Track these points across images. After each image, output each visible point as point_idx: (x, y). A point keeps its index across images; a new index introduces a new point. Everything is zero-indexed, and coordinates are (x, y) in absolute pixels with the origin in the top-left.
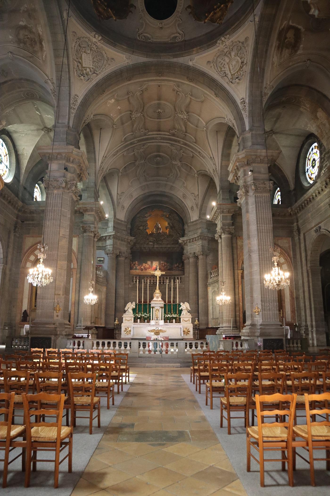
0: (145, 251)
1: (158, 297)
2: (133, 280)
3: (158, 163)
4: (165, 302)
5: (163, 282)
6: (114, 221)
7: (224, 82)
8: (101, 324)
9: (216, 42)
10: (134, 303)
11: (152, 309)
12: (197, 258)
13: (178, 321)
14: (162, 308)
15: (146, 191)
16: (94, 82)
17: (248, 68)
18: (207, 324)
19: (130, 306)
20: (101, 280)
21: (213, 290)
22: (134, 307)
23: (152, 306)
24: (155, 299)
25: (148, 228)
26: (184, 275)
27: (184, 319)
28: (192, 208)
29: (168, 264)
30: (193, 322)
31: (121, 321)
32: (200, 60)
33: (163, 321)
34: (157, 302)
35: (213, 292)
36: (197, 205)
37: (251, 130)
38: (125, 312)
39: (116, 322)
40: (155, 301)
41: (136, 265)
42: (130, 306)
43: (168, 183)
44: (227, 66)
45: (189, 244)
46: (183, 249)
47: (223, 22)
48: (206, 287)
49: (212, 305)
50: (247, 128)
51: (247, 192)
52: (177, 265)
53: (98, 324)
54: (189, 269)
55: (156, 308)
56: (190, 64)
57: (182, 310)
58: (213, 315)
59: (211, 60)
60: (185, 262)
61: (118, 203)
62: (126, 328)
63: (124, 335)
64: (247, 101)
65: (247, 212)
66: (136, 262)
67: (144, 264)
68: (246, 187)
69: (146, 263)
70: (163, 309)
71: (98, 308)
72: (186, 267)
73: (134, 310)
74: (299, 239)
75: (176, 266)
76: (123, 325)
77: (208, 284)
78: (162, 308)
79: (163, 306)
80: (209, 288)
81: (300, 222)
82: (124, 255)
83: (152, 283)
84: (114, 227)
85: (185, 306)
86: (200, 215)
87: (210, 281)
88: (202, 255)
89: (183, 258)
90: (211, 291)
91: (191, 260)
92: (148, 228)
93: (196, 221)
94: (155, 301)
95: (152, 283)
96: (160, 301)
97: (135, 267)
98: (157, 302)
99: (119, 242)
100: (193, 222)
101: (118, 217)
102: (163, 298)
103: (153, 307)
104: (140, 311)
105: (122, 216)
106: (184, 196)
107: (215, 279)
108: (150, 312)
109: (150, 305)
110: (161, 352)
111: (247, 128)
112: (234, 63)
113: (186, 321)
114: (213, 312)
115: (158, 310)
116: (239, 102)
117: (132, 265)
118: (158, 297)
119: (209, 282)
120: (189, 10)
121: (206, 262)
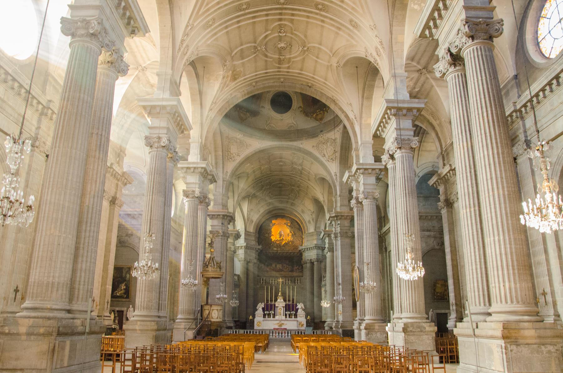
3: (280, 187)
6: (245, 234)
7: (323, 160)
9: (317, 136)
10: (263, 304)
12: (312, 263)
13: (296, 316)
15: (271, 206)
16: (238, 161)
17: (338, 155)
19: (260, 306)
23: (276, 305)
24: (278, 300)
25: (273, 235)
26: (302, 276)
28: (309, 222)
30: (306, 317)
31: (254, 317)
32: (307, 145)
34: (280, 303)
36: (313, 220)
37: (340, 196)
38: (257, 310)
39: (251, 317)
42: (260, 306)
43: (290, 200)
44: (325, 150)
45: (307, 252)
46: (301, 255)
47: (322, 122)
48: (320, 288)
50: (338, 193)
51: (336, 237)
54: (307, 273)
56: (301, 146)
57: (298, 309)
59: (315, 145)
61: (248, 219)
63: (256, 327)
64: (338, 174)
65: (336, 250)
68: (336, 234)
72: (304, 270)
73: (263, 309)
74: (386, 255)
76: (255, 320)
81: (387, 243)
84: (245, 239)
85: (300, 306)
86: (315, 227)
88: (317, 261)
91: (308, 265)
92: (273, 235)
93: (312, 233)
98: (280, 303)
99: (248, 251)
100: (310, 233)
101: (248, 230)
102: (285, 300)
105: (251, 229)
106: (303, 212)
109: (275, 305)
110: (282, 336)
111: (338, 193)
112: (329, 149)
116: (333, 174)
120: (301, 109)
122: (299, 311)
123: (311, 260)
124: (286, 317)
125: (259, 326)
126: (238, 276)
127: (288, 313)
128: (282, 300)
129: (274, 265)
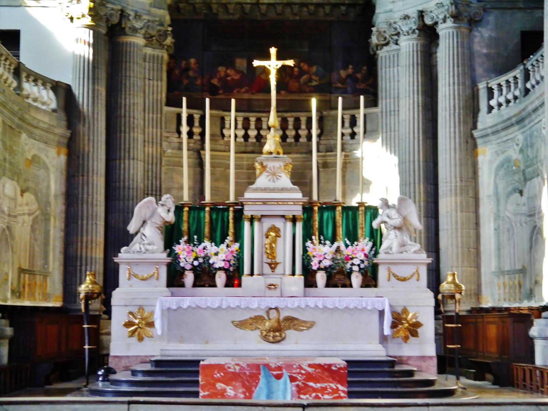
0: (226, 17)
1: (274, 175)
2: (179, 123)
4: (308, 193)
5: (297, 137)
8: (46, 297)
11: (246, 225)
12: (428, 34)
14: (294, 220)
18: (478, 294)
19: (149, 217)
20: (46, 119)
21: (501, 158)
22: (171, 217)
23: (248, 211)
24: (262, 181)
27: (396, 270)
29: (314, 69)
33: (299, 279)
35: (502, 165)
38: (127, 239)
40: (265, 190)
41: (191, 73)
48: (470, 146)
49: (497, 217)
52: (350, 71)
53: (32, 296)
55: (267, 223)
58: (499, 256)
60: (382, 53)
62: (135, 310)
63: (120, 344)
66: (192, 61)
67: (222, 69)
69: (231, 65)
70: (299, 226)
71: (33, 229)
73: (171, 235)
75: (343, 73)
76: (117, 296)
77: (476, 134)
78: (294, 220)
79: (298, 210)
80: (480, 149)
82: (138, 25)
83: (252, 140)
87: (485, 120)
88: (456, 17)
89: (374, 40)
90: (491, 162)
91: (409, 45)
94: (265, 190)
95: (252, 140)
96: (283, 190)
97: (185, 82)
103: (252, 220)
104: (195, 236)
107: (513, 110)
108: (238, 237)
113: (404, 280)
114: (499, 249)
115: (276, 230)
117: (177, 72)
118: (274, 175)
119: (480, 125)
121: (470, 49)
122: (391, 240)
123: (421, 14)
124: (310, 282)
125: (140, 327)
126: (63, 91)
127: (322, 253)
128: (285, 181)
129: (240, 63)
